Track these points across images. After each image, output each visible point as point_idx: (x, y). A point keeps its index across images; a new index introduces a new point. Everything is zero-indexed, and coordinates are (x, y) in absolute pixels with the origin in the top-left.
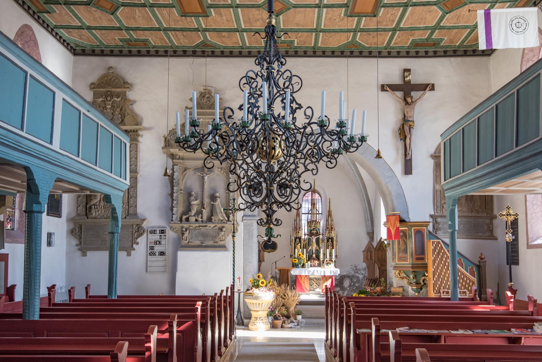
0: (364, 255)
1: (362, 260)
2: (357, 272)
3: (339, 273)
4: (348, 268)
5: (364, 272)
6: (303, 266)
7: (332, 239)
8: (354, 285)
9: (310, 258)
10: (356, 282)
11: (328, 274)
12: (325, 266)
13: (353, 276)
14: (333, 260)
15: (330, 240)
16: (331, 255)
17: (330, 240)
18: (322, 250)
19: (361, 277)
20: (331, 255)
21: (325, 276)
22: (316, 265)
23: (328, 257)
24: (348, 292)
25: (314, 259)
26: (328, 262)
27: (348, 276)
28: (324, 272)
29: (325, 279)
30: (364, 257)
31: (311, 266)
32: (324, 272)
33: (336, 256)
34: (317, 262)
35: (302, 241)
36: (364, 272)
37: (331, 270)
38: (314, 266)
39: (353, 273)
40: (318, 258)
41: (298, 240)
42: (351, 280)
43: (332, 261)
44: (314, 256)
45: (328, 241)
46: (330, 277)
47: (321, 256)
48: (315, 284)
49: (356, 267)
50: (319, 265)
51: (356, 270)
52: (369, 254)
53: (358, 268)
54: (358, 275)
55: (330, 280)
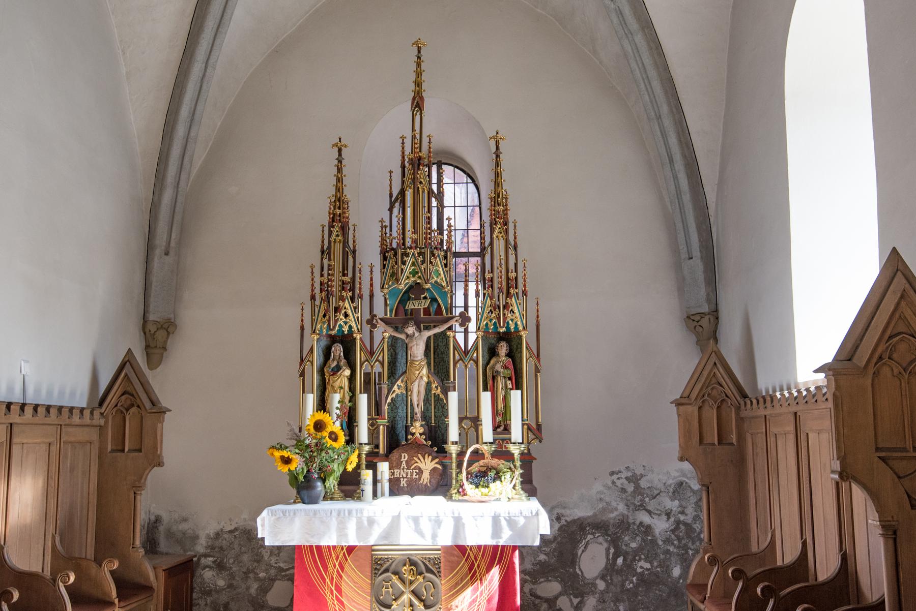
0: (684, 420)
1: (674, 446)
2: (642, 507)
3: (544, 526)
4: (598, 487)
5: (673, 505)
6: (350, 486)
7: (511, 338)
8: (629, 567)
9: (394, 442)
10: (637, 552)
11: (478, 536)
12: (468, 487)
13: (624, 524)
14: (515, 451)
15: (503, 349)
16: (502, 426)
17: (503, 349)
18: (453, 397)
19: (661, 526)
20: (502, 426)
21: (462, 549)
22: (426, 476)
23: (487, 433)
24: (602, 601)
25: (416, 448)
26: (489, 461)
27: (599, 526)
28: (458, 523)
29: (463, 566)
30: (685, 435)
31: (395, 489)
32: (458, 523)
33: (534, 430)
34: (427, 464)
35: (359, 356)
36: (673, 505)
37: (502, 513)
38: (414, 489)
39: (621, 508)
40: (436, 439)
41: (338, 350)
42: (615, 542)
43: (509, 456)
44: (418, 428)
45: (492, 352)
46: (497, 555)
47: (453, 433)
48: (407, 597)
49: (634, 479)
50: (442, 485)
51: (638, 493)
52: (711, 415)
53: (643, 483)
54: (645, 518)
55: (495, 574)
